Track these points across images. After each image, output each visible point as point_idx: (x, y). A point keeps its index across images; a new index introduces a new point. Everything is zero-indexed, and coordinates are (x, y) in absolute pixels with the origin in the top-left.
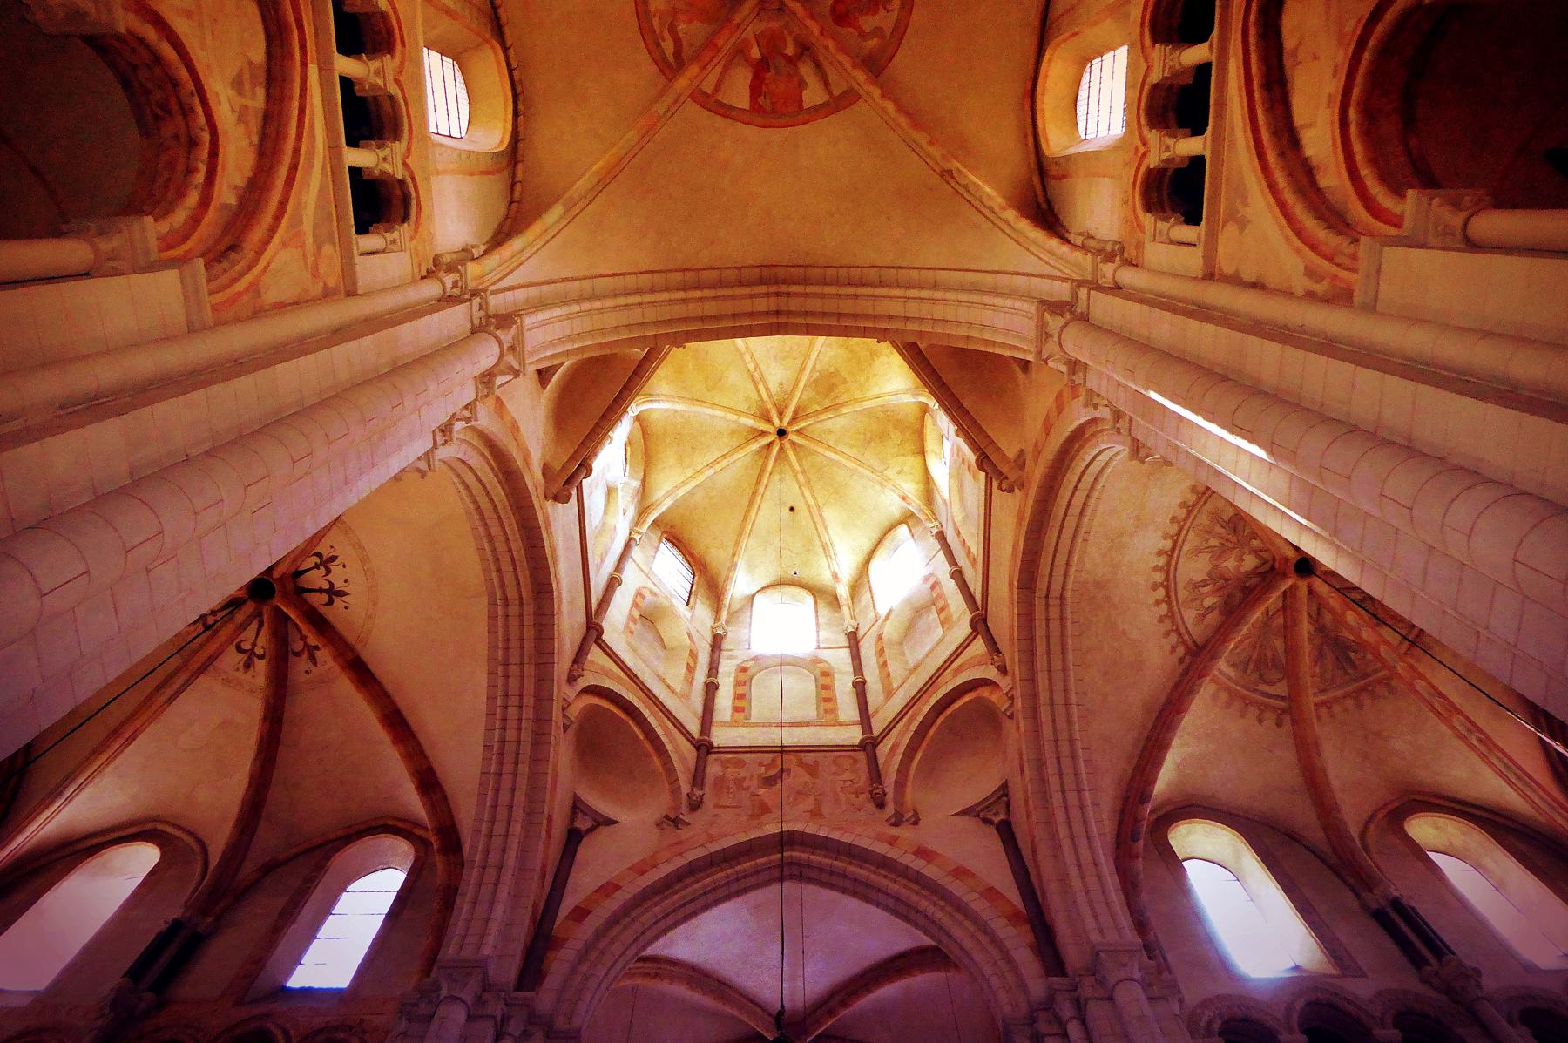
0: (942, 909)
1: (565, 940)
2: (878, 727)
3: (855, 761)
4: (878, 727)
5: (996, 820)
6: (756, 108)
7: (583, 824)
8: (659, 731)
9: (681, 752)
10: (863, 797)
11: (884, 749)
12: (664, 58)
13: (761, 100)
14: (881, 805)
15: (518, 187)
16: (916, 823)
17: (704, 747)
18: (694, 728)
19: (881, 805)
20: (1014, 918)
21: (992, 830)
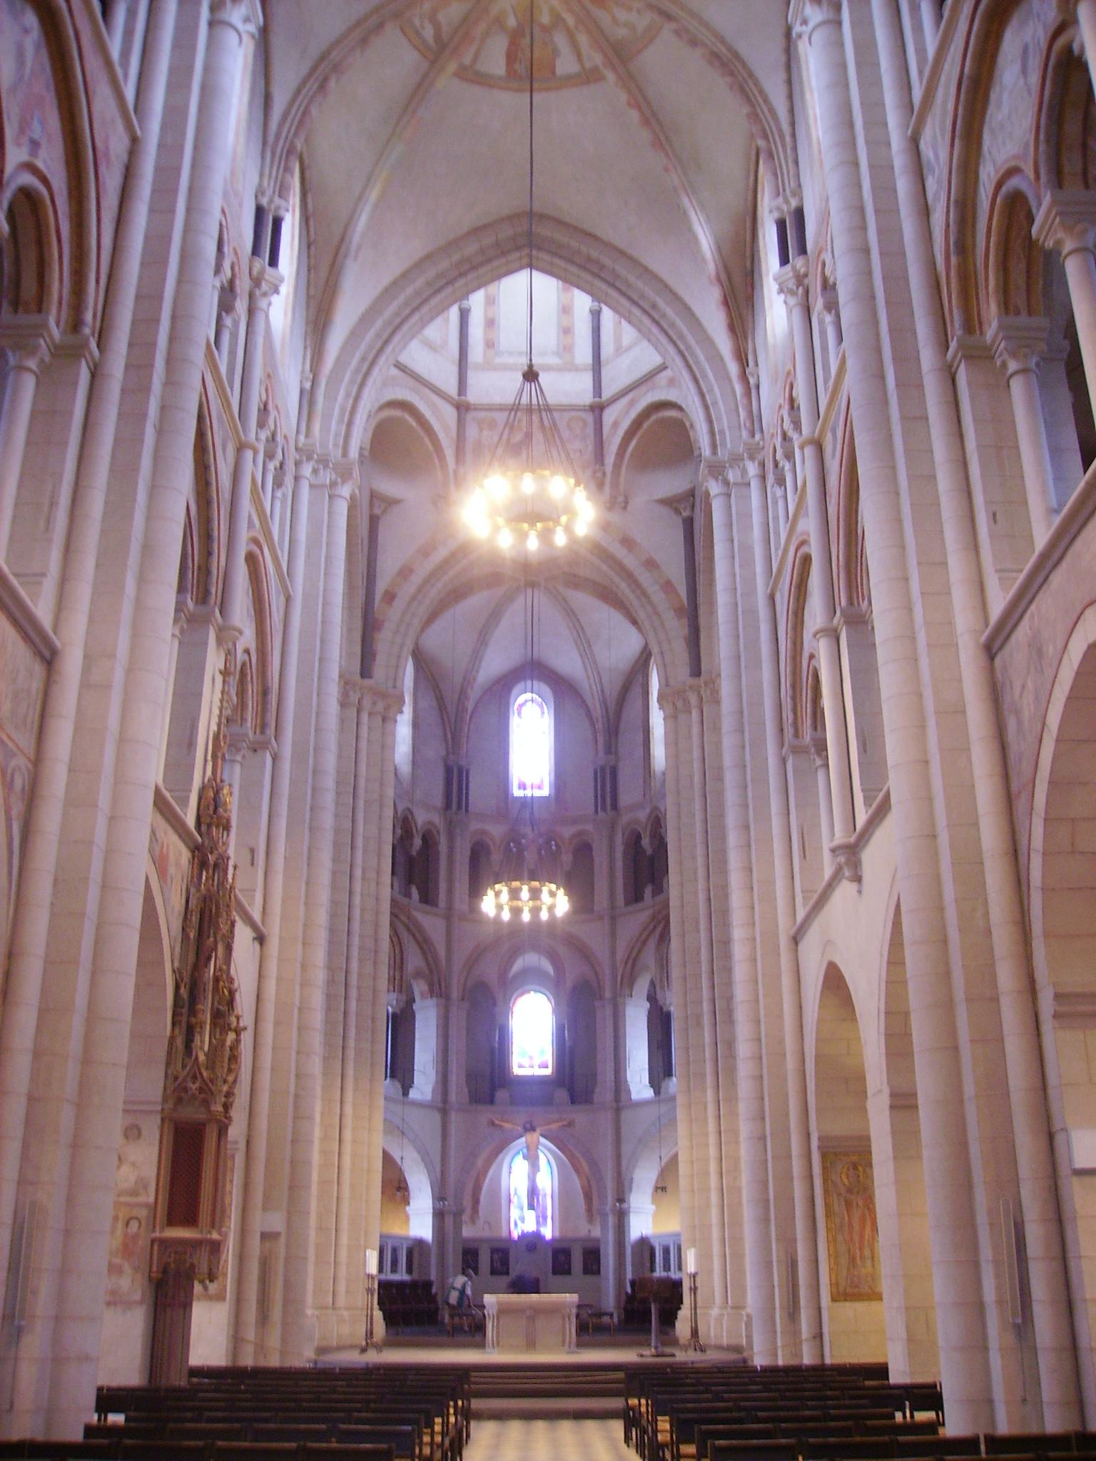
0: (633, 591)
1: (383, 622)
2: (607, 394)
4: (607, 394)
5: (686, 514)
6: (511, 73)
7: (377, 511)
9: (442, 418)
11: (609, 416)
12: (424, 42)
13: (517, 66)
15: (312, 223)
16: (625, 508)
17: (462, 408)
20: (679, 611)
21: (678, 522)
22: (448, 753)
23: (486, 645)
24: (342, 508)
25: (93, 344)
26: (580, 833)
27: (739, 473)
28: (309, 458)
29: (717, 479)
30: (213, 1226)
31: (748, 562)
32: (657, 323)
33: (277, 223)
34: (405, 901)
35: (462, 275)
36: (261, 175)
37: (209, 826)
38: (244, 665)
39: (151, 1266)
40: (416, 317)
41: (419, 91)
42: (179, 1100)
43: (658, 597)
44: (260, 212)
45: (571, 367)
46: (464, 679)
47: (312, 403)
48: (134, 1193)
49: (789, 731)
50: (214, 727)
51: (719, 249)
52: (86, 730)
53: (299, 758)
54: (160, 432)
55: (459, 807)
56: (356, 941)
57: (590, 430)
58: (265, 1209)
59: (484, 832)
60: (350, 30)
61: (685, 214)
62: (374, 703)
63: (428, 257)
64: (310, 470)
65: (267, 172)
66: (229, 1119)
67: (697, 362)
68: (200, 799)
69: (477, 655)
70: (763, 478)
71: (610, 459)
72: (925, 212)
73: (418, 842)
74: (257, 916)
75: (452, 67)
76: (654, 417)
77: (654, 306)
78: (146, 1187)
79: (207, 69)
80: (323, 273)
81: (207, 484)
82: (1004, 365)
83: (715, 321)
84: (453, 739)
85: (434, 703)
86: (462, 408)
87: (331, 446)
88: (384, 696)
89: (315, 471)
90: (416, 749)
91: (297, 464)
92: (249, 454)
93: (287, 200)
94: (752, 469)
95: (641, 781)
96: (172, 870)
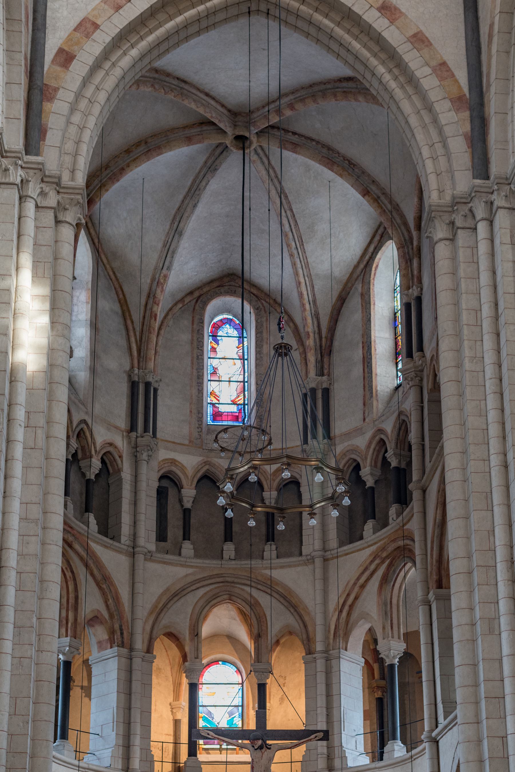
23: (181, 234)
46: (153, 279)
55: (146, 429)
85: (117, 307)
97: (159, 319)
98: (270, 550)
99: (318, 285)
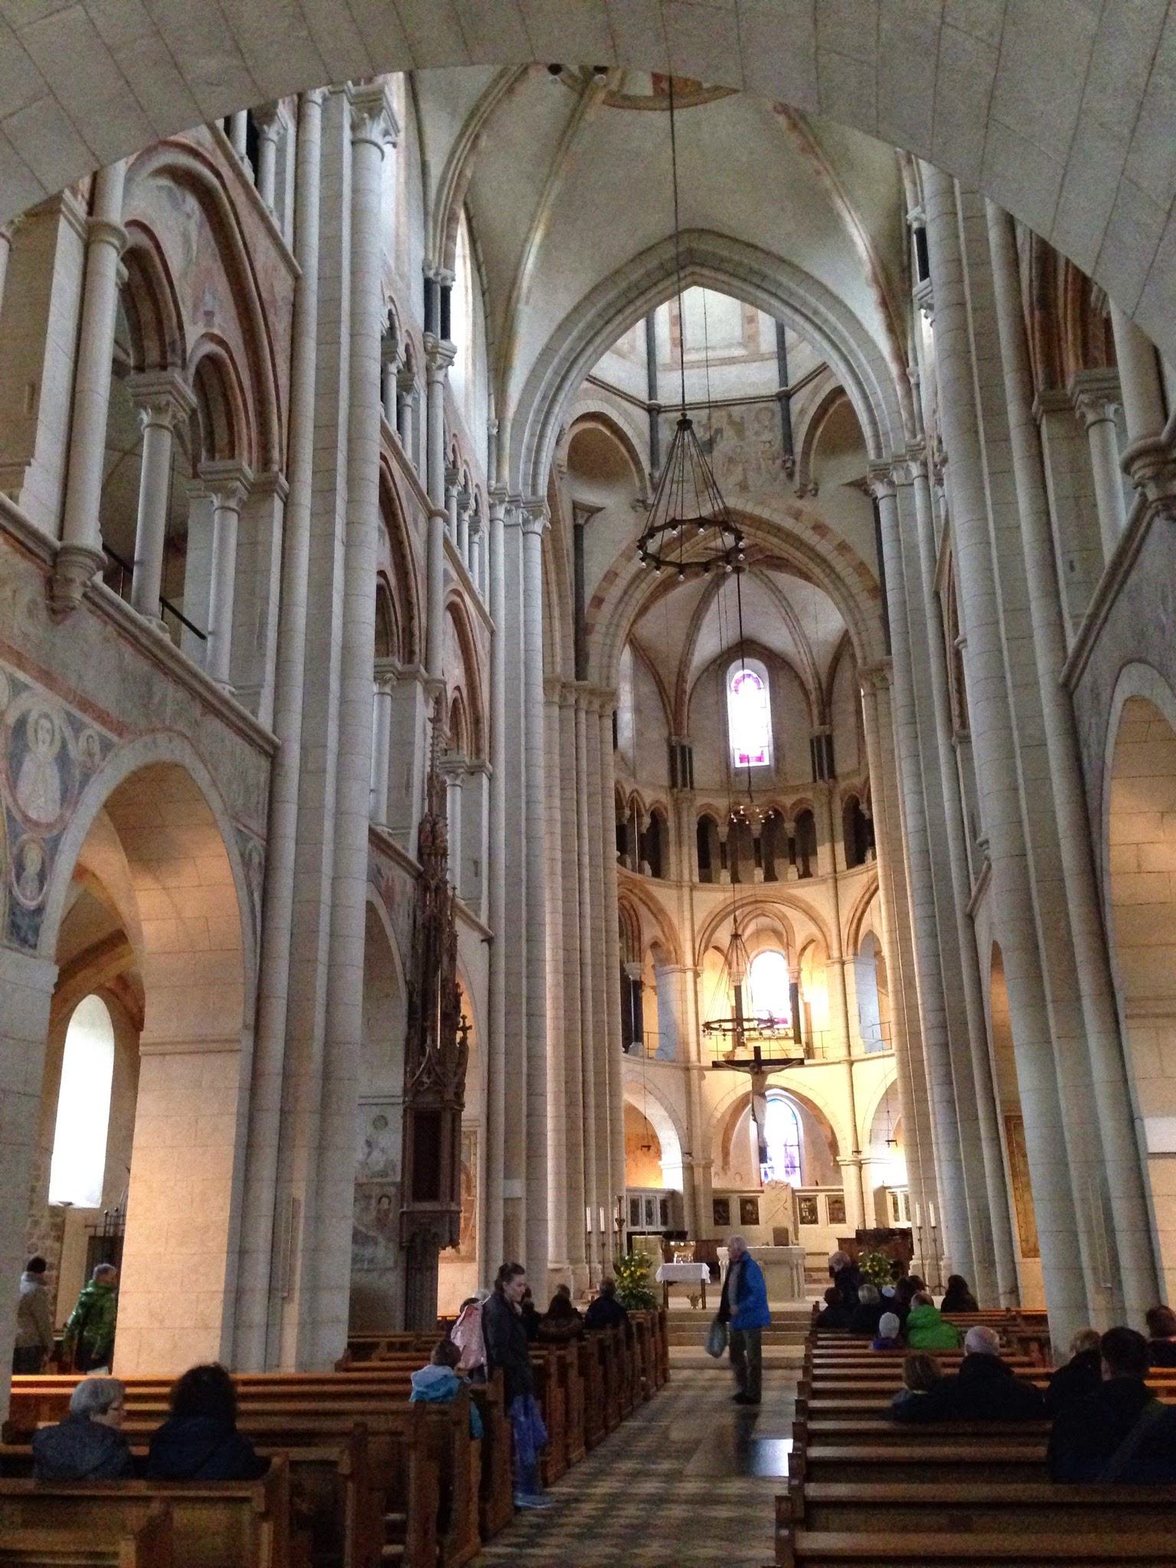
1: (593, 626)
2: (792, 382)
3: (773, 415)
4: (792, 382)
7: (581, 521)
8: (621, 422)
9: (634, 424)
10: (779, 462)
11: (796, 404)
14: (790, 475)
16: (815, 495)
17: (654, 411)
18: (643, 396)
19: (790, 475)
22: (670, 734)
24: (536, 542)
25: (282, 478)
26: (801, 801)
27: (902, 473)
28: (502, 502)
29: (882, 481)
30: (452, 1199)
31: (913, 561)
32: (820, 329)
33: (446, 292)
34: (638, 876)
35: (631, 302)
36: (426, 248)
37: (429, 855)
38: (455, 701)
39: (401, 1237)
40: (591, 349)
41: (573, 119)
42: (417, 1093)
43: (852, 579)
44: (428, 284)
45: (756, 357)
46: (681, 662)
47: (500, 448)
48: (384, 1174)
49: (956, 721)
50: (428, 769)
51: (875, 248)
52: (309, 810)
53: (513, 775)
54: (348, 545)
55: (684, 785)
56: (588, 922)
57: (778, 420)
58: (506, 1177)
59: (709, 805)
60: (496, 82)
61: (839, 216)
62: (590, 703)
63: (594, 290)
64: (503, 511)
65: (431, 245)
66: (462, 1105)
67: (860, 366)
68: (420, 832)
69: (691, 640)
70: (926, 477)
71: (798, 447)
72: (1014, 264)
73: (647, 820)
74: (483, 920)
75: (601, 96)
76: (838, 402)
77: (816, 312)
78: (393, 1169)
79: (356, 190)
80: (500, 321)
81: (404, 557)
82: (1083, 416)
83: (874, 322)
84: (675, 720)
85: (656, 689)
86: (654, 411)
87: (521, 487)
88: (601, 694)
89: (508, 512)
90: (639, 733)
91: (491, 507)
92: (439, 521)
93: (452, 270)
94: (915, 469)
95: (855, 751)
96: (398, 898)
97: (688, 691)
98: (792, 872)
99: (815, 650)
